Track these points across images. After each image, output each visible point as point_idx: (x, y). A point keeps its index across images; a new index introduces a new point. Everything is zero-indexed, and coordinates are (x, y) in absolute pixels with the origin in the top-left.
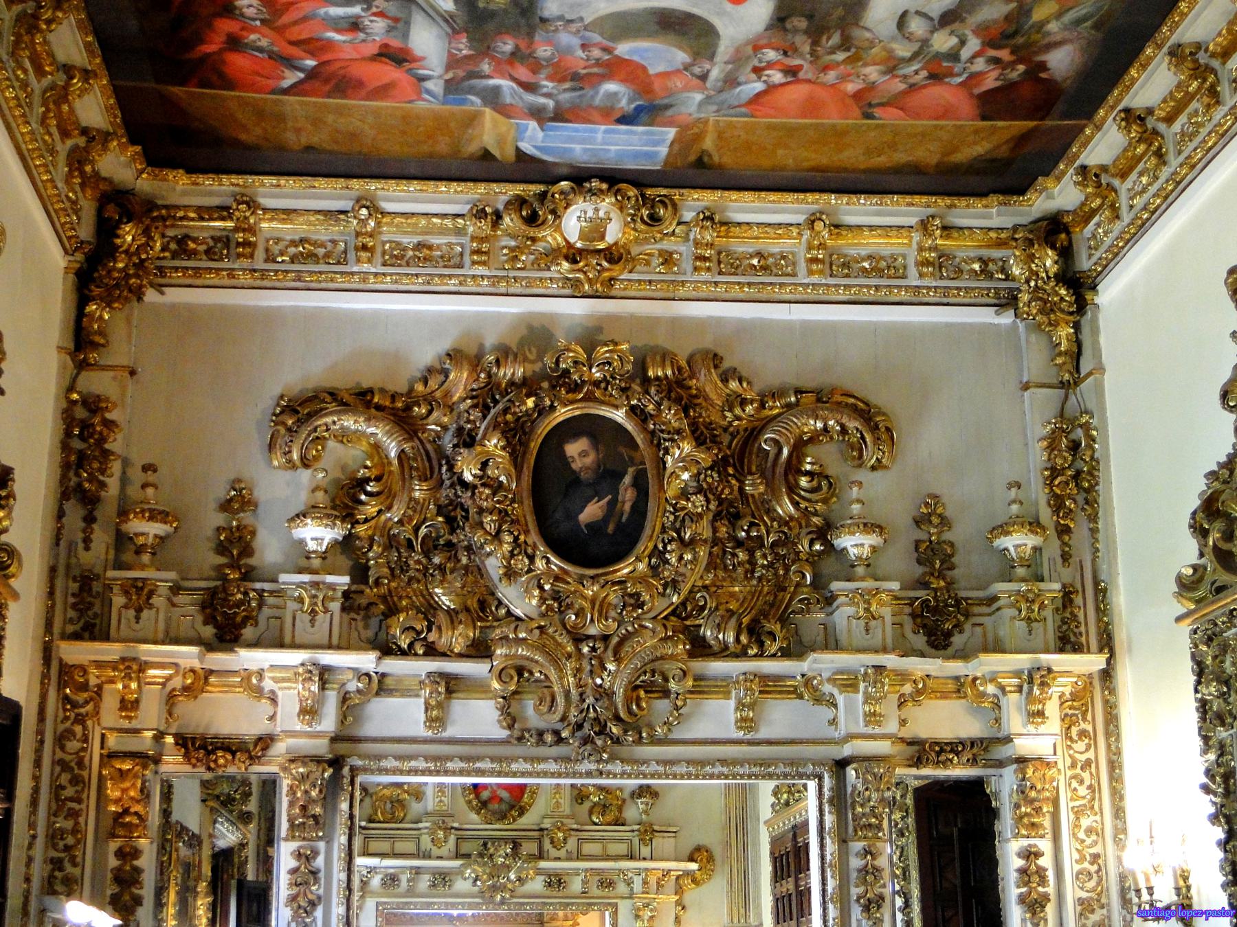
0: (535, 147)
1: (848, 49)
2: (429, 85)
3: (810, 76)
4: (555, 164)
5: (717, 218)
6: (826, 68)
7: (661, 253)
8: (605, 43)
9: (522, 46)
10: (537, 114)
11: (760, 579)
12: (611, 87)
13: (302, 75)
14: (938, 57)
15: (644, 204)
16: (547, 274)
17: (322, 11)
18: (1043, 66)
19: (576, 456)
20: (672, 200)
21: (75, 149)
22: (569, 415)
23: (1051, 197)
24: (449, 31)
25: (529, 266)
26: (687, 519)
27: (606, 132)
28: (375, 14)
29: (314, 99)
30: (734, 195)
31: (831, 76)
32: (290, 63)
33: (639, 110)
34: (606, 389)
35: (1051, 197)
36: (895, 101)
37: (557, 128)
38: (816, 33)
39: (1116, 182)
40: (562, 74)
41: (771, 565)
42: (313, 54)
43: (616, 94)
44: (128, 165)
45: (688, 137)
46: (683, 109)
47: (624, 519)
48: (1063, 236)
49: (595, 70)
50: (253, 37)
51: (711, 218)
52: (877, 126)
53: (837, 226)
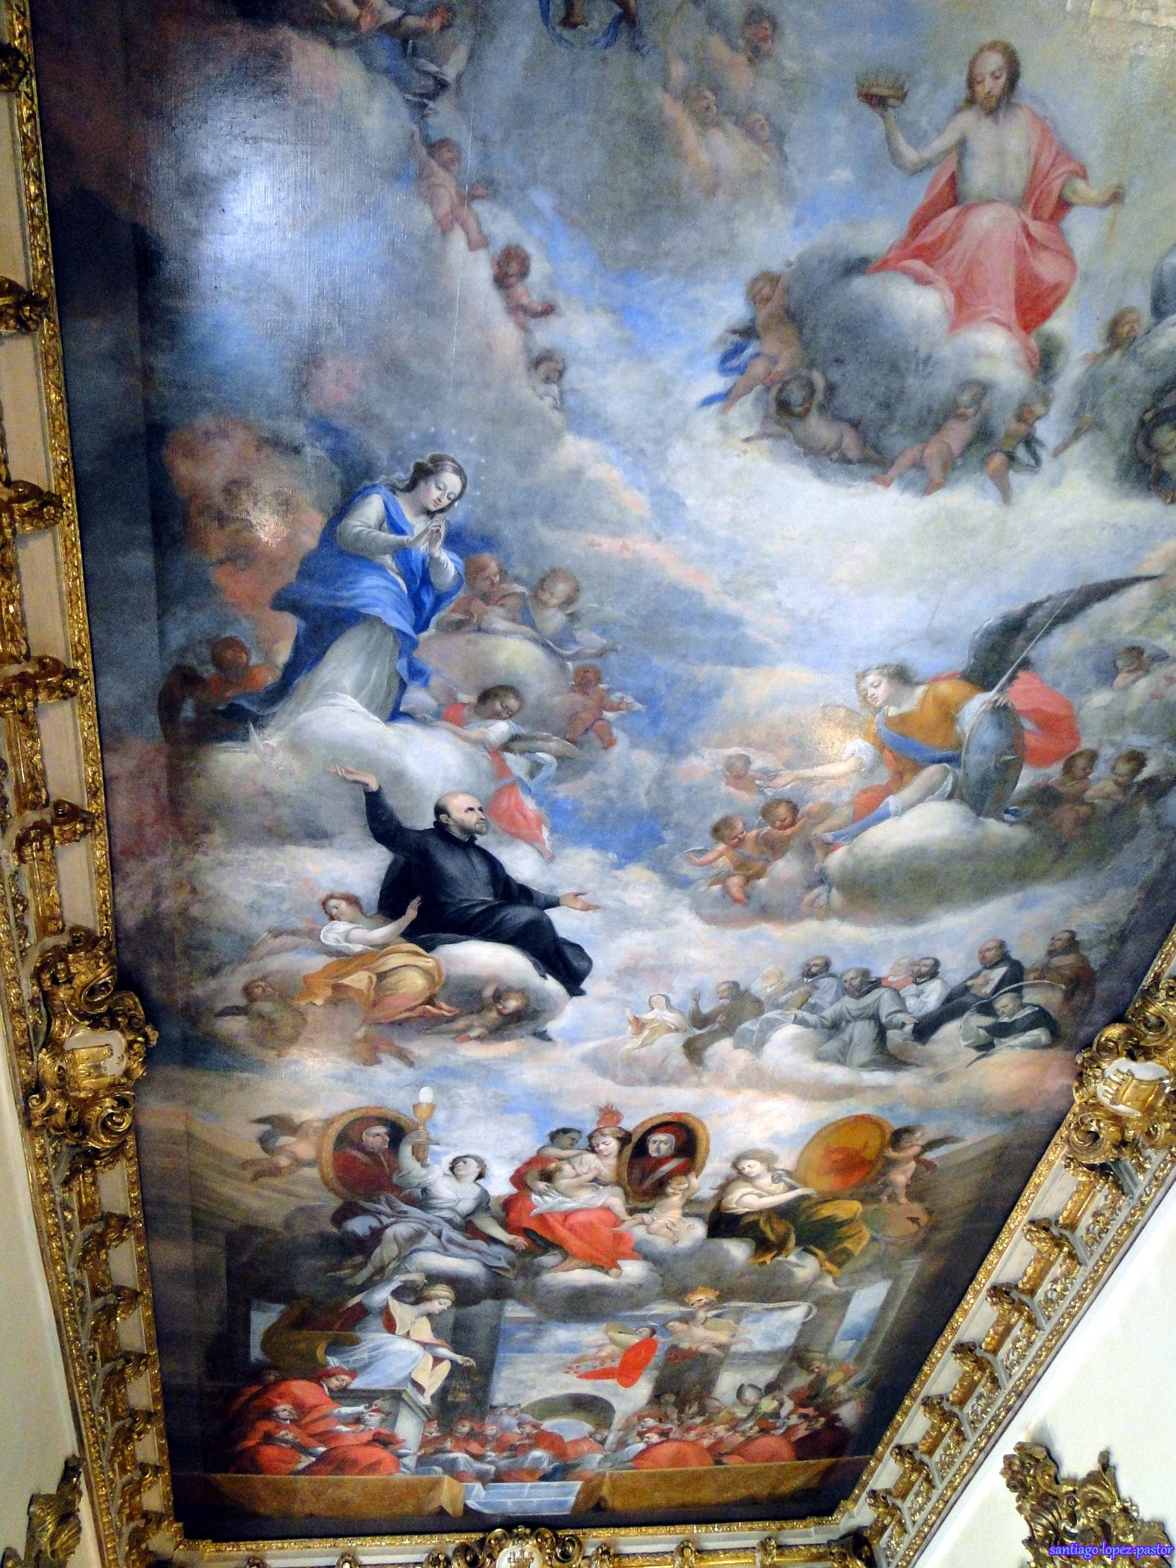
1: (703, 1415)
2: (406, 1461)
3: (677, 1436)
4: (494, 1515)
5: (612, 1552)
6: (689, 1429)
8: (534, 1421)
9: (476, 1429)
10: (482, 1477)
12: (537, 1453)
13: (314, 1459)
14: (766, 1416)
15: (557, 1543)
17: (336, 1411)
18: (836, 1418)
20: (578, 1539)
21: (136, 1530)
23: (852, 1516)
24: (425, 1419)
27: (531, 1488)
28: (374, 1411)
29: (318, 1477)
30: (623, 1531)
31: (692, 1435)
32: (305, 1450)
33: (555, 1470)
35: (852, 1516)
36: (737, 1451)
37: (494, 1488)
38: (681, 1405)
39: (899, 1502)
40: (503, 1446)
42: (324, 1443)
43: (540, 1458)
44: (170, 1539)
45: (590, 1490)
46: (587, 1466)
48: (866, 1548)
49: (526, 1442)
50: (282, 1433)
51: (606, 1552)
53: (699, 1551)
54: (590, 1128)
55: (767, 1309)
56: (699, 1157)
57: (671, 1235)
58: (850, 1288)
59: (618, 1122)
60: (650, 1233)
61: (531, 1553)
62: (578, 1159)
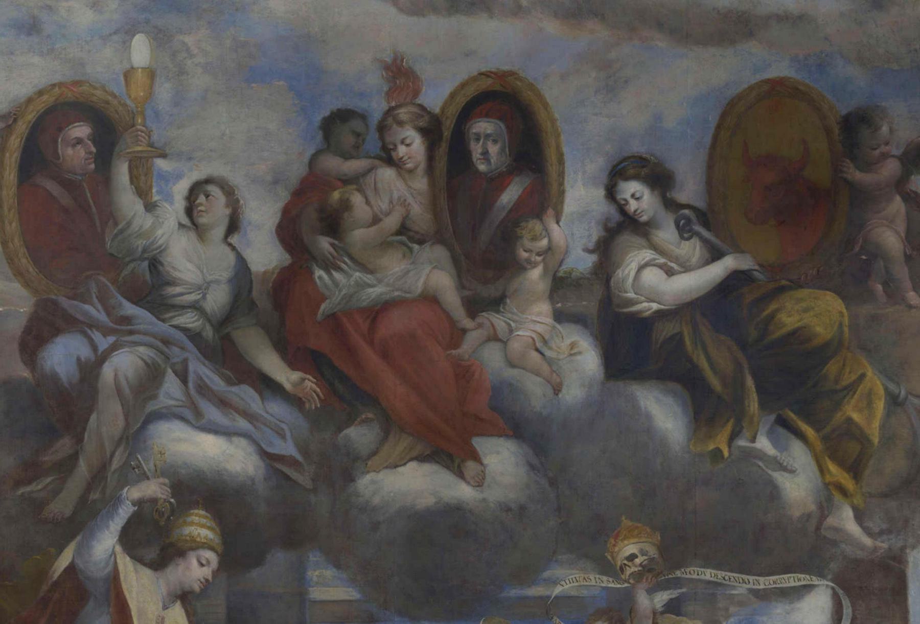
54: (377, 107)
55: (756, 593)
56: (552, 170)
57: (545, 368)
58: (896, 542)
59: (416, 93)
60: (512, 365)
62: (370, 179)
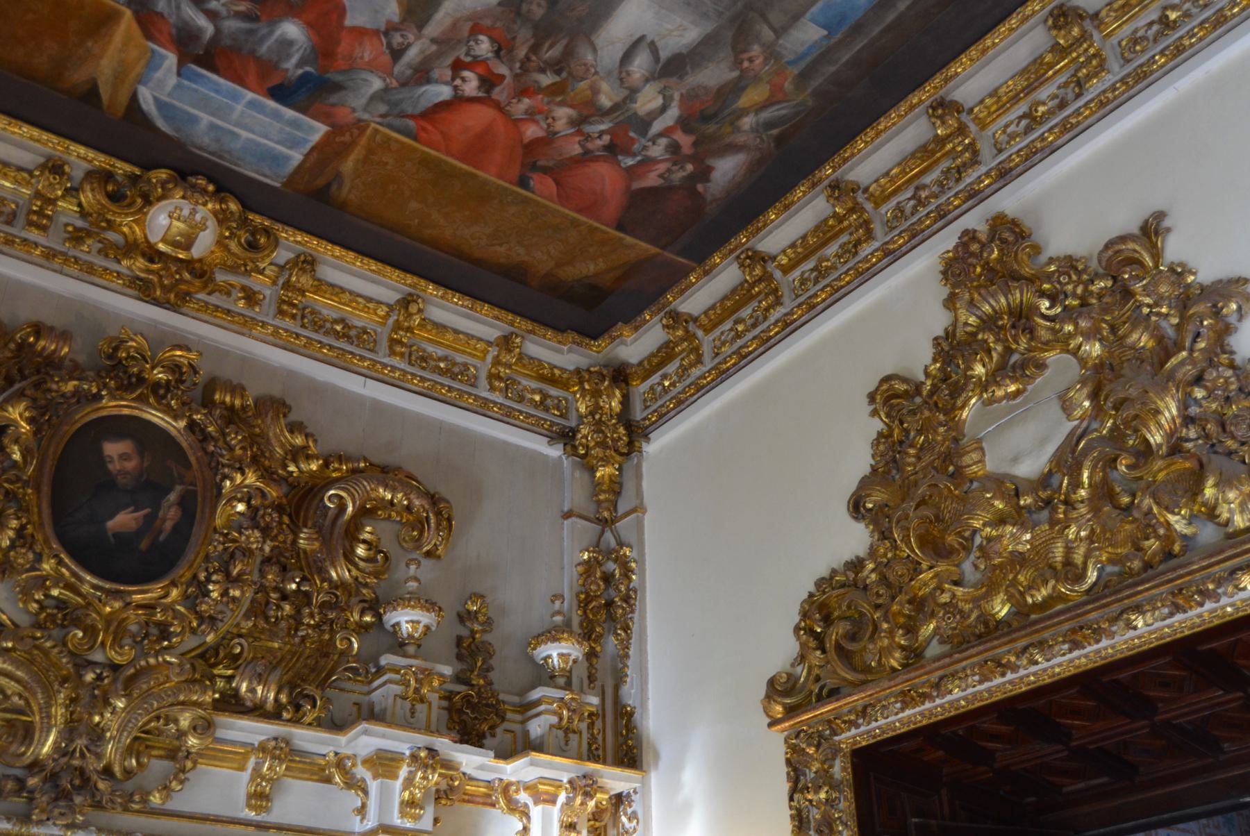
0: (156, 99)
1: (558, 72)
7: (244, 288)
11: (303, 639)
16: (114, 266)
19: (115, 457)
22: (115, 412)
25: (94, 251)
26: (238, 553)
27: (252, 104)
34: (164, 397)
41: (317, 626)
43: (290, 43)
47: (161, 538)
52: (526, 201)
61: (204, 219)
